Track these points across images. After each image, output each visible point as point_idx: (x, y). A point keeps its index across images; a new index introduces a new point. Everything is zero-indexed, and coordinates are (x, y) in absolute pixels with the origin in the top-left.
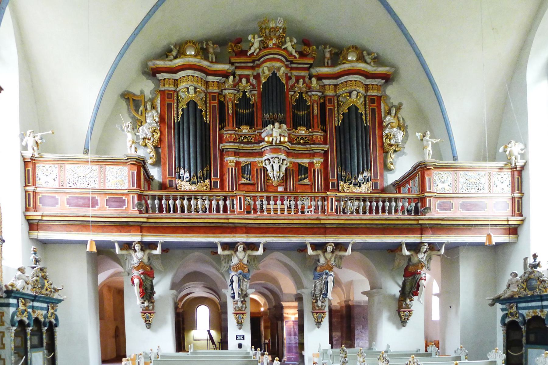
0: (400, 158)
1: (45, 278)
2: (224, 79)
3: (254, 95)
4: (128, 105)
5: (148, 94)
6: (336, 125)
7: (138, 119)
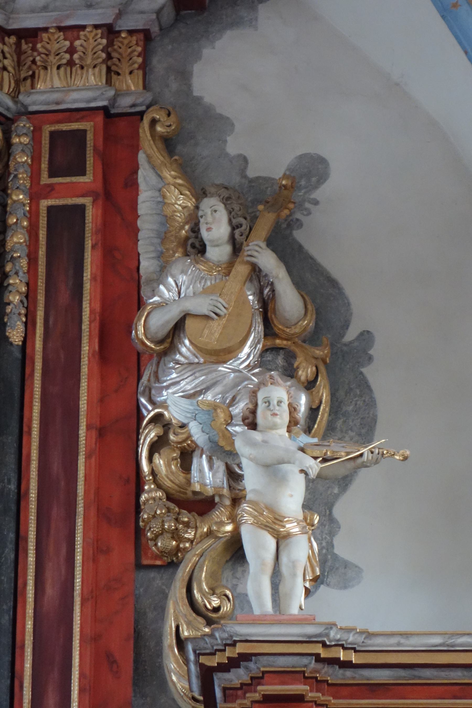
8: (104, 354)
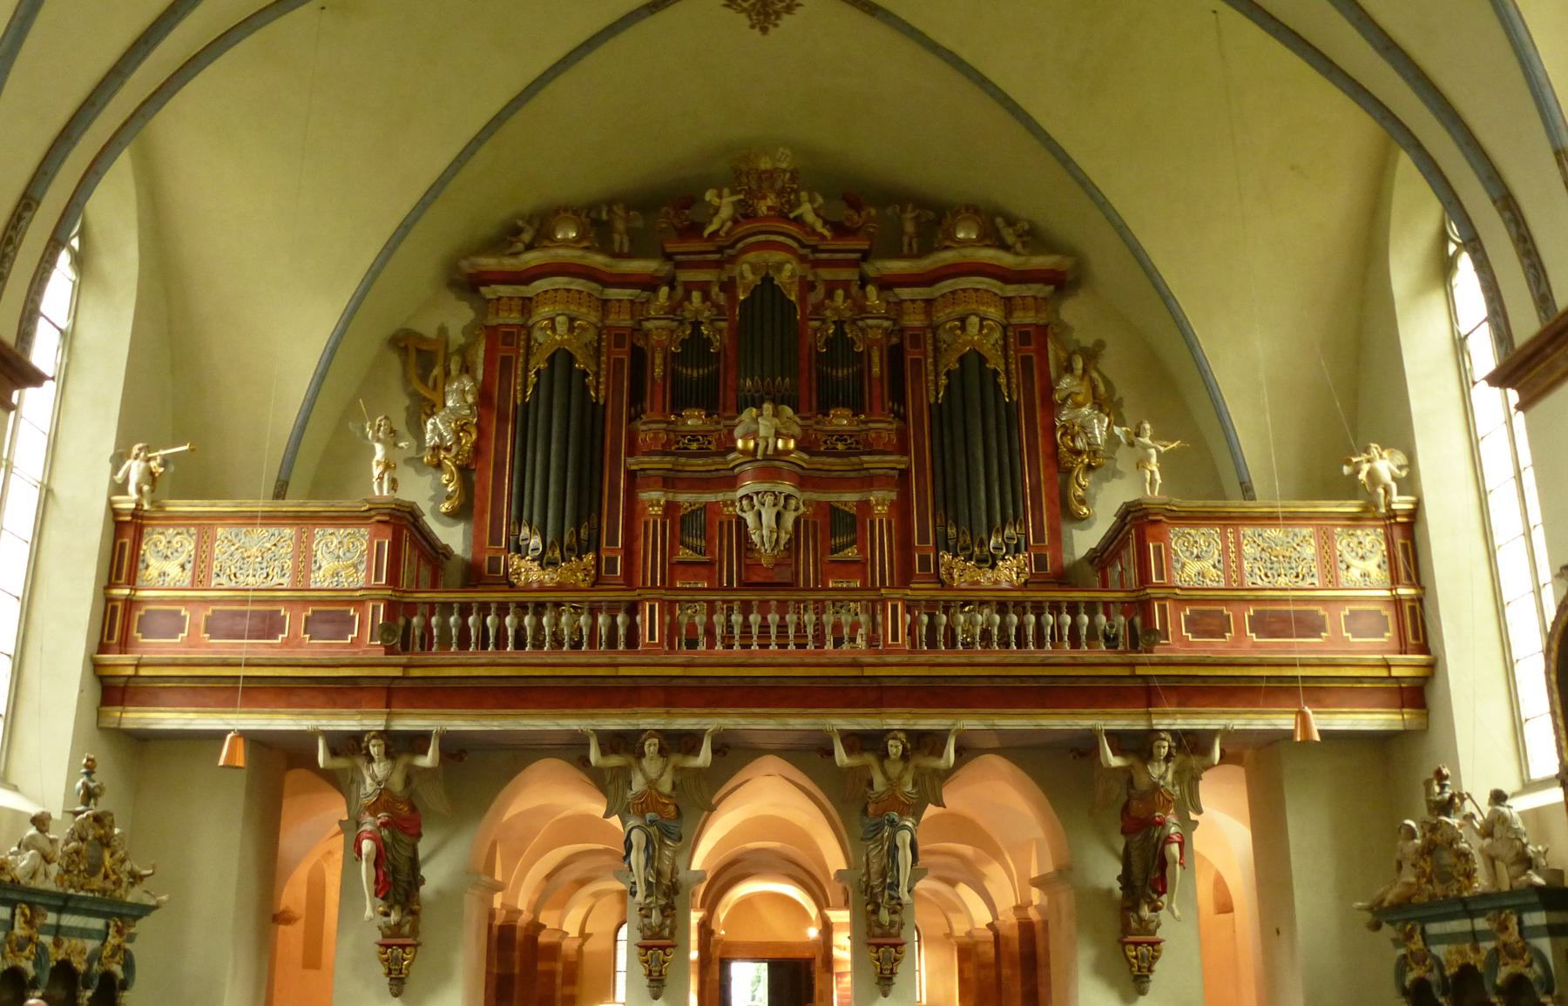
0: (1105, 485)
1: (105, 842)
2: (646, 294)
3: (720, 331)
4: (405, 364)
5: (457, 337)
6: (932, 400)
7: (425, 399)
8: (1042, 405)
